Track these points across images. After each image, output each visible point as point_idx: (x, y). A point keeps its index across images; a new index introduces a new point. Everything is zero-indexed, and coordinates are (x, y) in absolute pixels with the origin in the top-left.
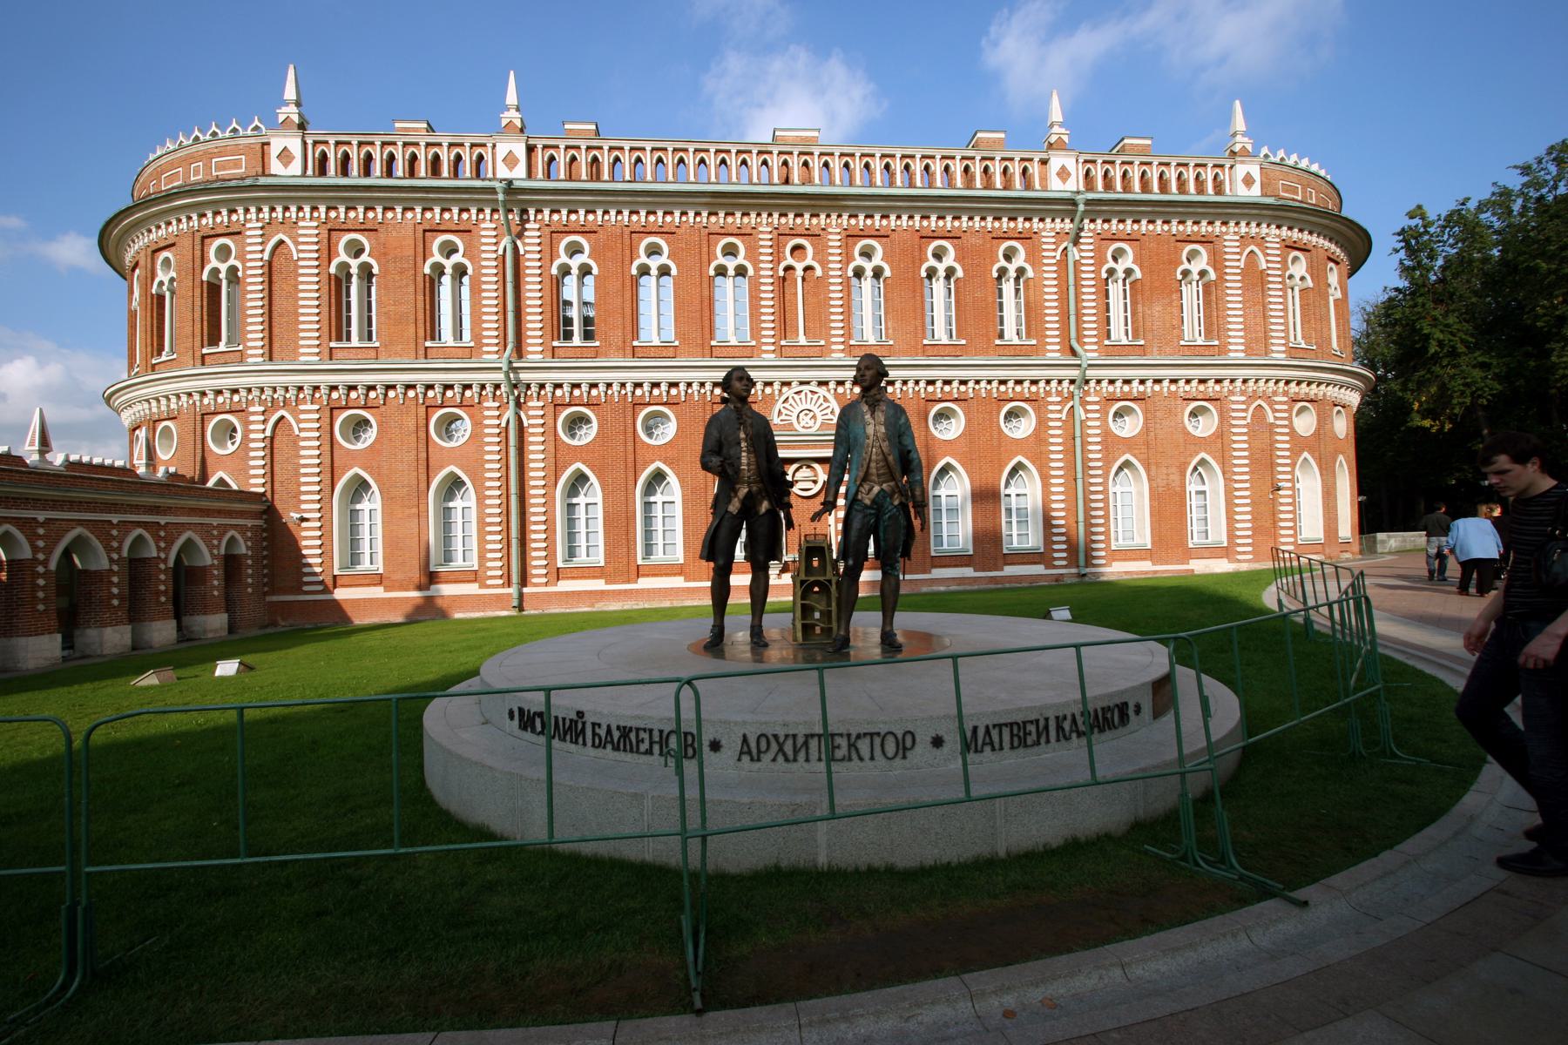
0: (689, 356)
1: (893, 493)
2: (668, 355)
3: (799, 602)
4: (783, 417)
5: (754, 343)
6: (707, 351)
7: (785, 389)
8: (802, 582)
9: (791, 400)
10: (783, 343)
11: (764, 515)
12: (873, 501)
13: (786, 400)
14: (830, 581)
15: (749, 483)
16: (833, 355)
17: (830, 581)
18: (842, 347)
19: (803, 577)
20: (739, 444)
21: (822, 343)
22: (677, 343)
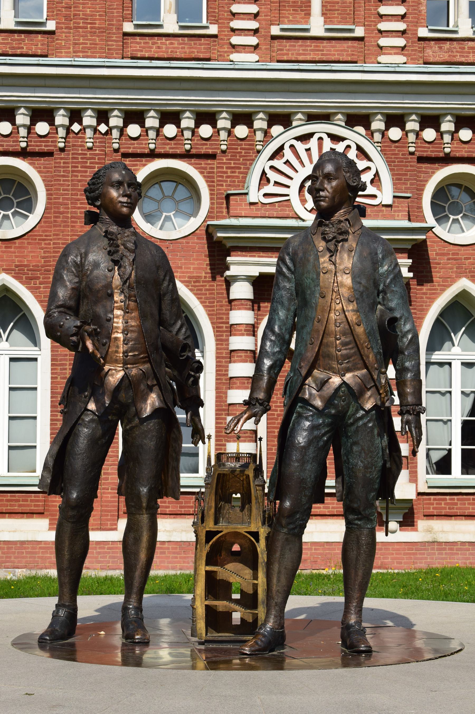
0: (76, 53)
1: (363, 389)
2: (33, 50)
3: (203, 569)
4: (270, 189)
5: (213, 30)
6: (115, 44)
7: (277, 130)
8: (210, 535)
9: (288, 154)
10: (275, 30)
11: (148, 418)
12: (329, 402)
13: (278, 152)
14: (256, 535)
15: (125, 363)
16: (382, 59)
17: (256, 535)
18: (401, 42)
19: (210, 525)
20: (111, 296)
21: (359, 32)
22: (51, 26)
